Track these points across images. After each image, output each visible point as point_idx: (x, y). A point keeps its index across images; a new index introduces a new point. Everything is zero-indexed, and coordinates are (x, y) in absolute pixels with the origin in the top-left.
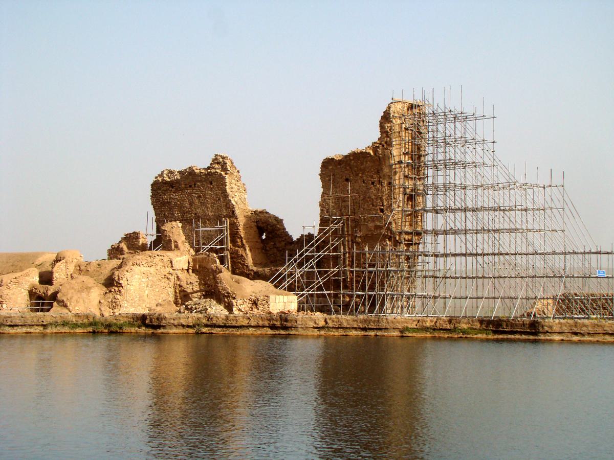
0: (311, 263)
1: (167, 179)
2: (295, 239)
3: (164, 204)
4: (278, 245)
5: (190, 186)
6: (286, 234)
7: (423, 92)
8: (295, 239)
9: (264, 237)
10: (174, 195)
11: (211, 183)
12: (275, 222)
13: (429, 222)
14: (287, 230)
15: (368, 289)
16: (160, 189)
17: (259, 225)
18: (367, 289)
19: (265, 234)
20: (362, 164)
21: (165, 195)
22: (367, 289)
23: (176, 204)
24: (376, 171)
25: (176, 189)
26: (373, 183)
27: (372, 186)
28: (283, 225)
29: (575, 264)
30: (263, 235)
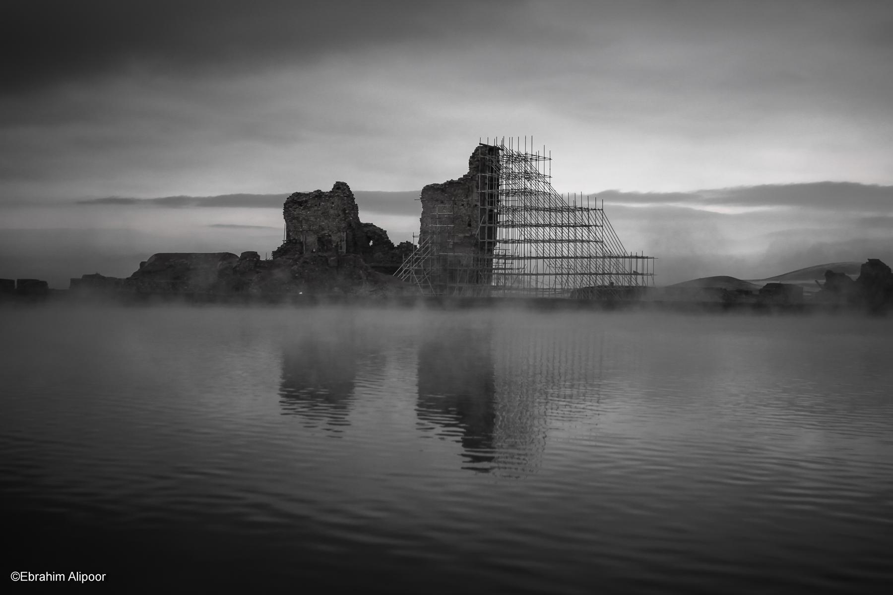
0: (419, 263)
2: (396, 246)
5: (316, 205)
6: (389, 242)
7: (503, 141)
8: (396, 246)
9: (371, 243)
12: (381, 233)
13: (502, 233)
14: (389, 239)
15: (459, 282)
16: (291, 207)
17: (368, 235)
18: (458, 281)
19: (372, 242)
20: (455, 191)
21: (295, 211)
22: (458, 281)
23: (304, 219)
24: (465, 196)
25: (304, 208)
26: (463, 205)
27: (462, 207)
28: (386, 235)
29: (626, 266)
30: (370, 242)
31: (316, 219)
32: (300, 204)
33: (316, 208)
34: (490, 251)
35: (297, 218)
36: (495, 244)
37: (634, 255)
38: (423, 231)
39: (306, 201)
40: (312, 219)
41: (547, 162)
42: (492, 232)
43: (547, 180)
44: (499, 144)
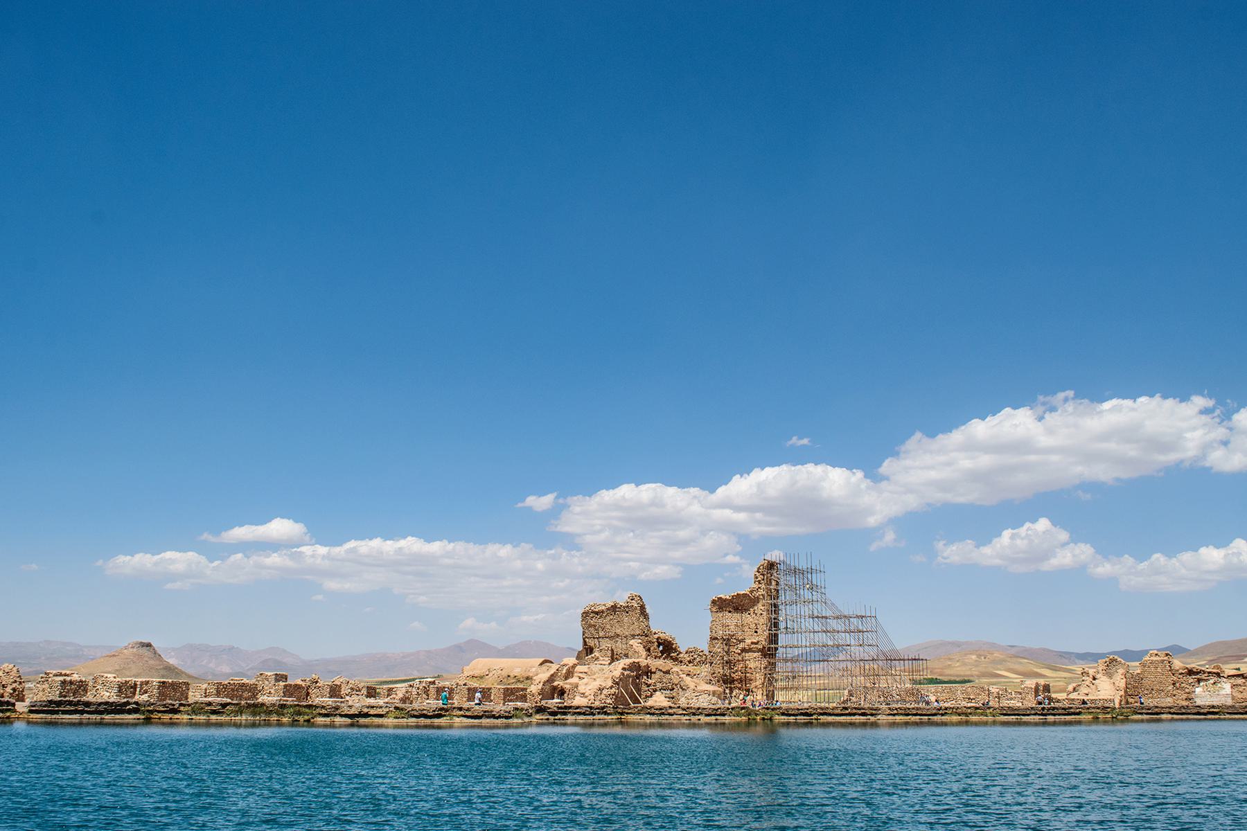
1: (592, 608)
3: (590, 626)
4: (672, 654)
9: (661, 648)
10: (600, 621)
11: (627, 613)
26: (749, 614)
31: (612, 627)
32: (597, 613)
33: (612, 617)
34: (773, 656)
35: (595, 626)
36: (776, 649)
37: (914, 658)
38: (713, 639)
39: (603, 612)
40: (608, 626)
41: (822, 574)
42: (773, 639)
43: (823, 590)
44: (778, 562)
